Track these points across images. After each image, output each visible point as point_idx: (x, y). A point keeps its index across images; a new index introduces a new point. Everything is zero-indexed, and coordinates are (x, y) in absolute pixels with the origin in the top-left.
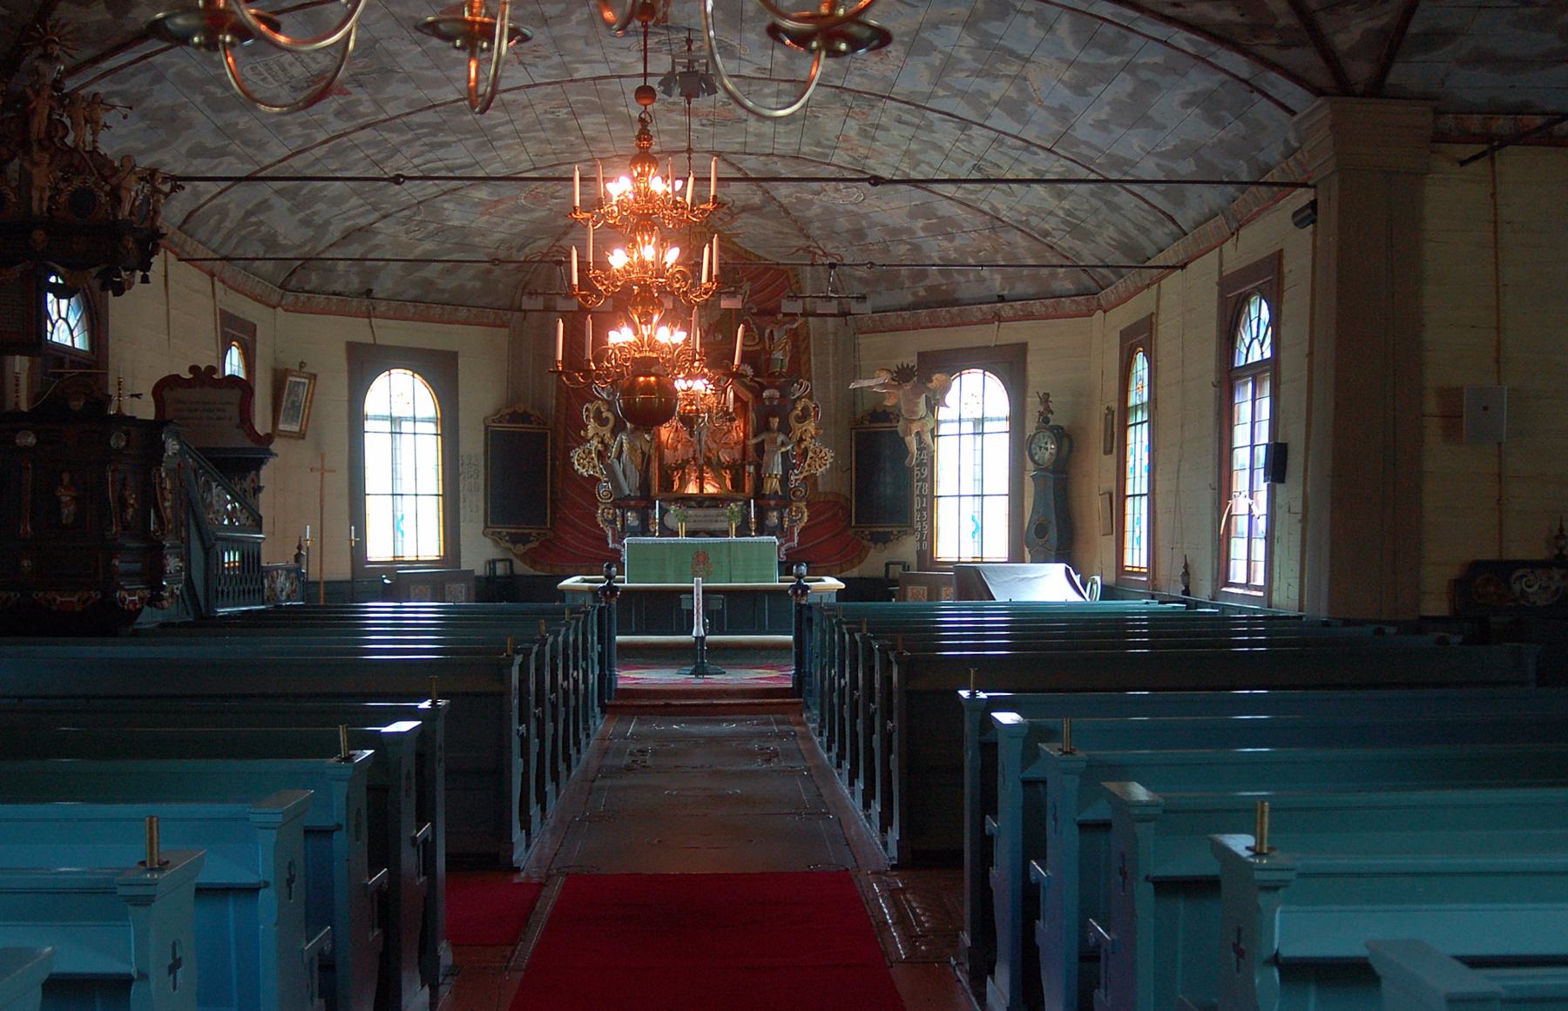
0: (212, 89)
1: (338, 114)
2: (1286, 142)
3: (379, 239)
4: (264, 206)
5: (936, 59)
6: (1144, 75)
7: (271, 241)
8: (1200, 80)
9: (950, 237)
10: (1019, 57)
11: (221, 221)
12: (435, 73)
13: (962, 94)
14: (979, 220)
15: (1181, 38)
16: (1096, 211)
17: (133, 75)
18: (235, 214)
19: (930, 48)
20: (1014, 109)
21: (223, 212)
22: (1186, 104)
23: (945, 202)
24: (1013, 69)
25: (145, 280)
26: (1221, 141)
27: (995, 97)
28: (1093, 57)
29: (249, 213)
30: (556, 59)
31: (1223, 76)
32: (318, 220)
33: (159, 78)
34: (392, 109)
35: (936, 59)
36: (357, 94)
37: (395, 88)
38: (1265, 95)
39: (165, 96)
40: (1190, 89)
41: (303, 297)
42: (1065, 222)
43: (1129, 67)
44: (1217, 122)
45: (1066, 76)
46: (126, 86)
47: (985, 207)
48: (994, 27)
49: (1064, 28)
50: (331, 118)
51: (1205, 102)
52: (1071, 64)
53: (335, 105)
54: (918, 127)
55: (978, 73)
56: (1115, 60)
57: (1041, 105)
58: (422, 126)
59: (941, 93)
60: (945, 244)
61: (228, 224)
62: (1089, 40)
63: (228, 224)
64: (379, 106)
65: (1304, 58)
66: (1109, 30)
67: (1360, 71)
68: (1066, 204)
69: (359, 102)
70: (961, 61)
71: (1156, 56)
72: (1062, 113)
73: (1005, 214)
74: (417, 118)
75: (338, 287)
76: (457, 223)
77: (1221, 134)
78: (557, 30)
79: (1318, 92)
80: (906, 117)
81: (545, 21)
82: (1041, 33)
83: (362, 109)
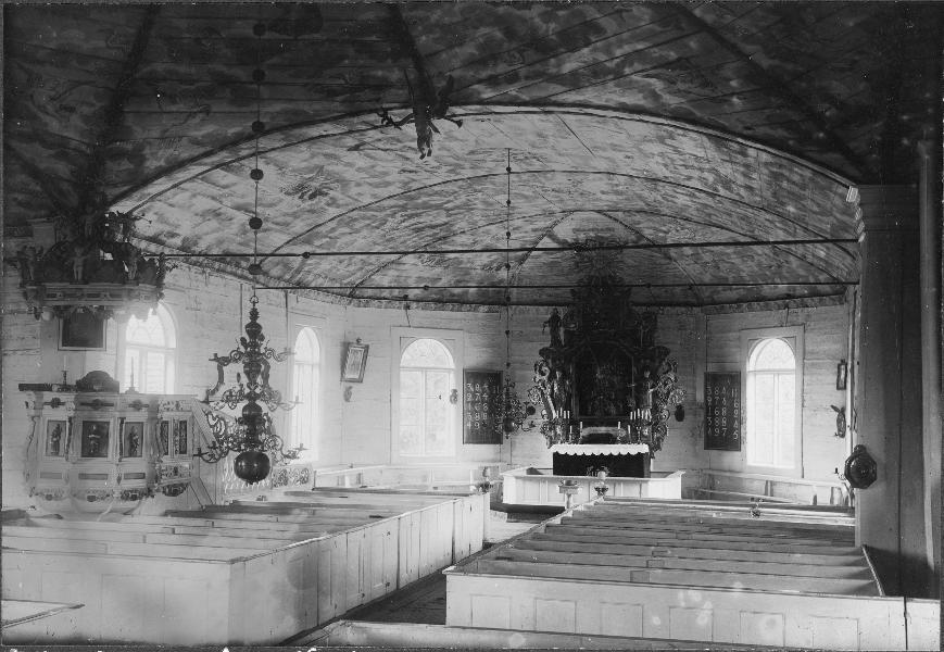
60: (750, 263)
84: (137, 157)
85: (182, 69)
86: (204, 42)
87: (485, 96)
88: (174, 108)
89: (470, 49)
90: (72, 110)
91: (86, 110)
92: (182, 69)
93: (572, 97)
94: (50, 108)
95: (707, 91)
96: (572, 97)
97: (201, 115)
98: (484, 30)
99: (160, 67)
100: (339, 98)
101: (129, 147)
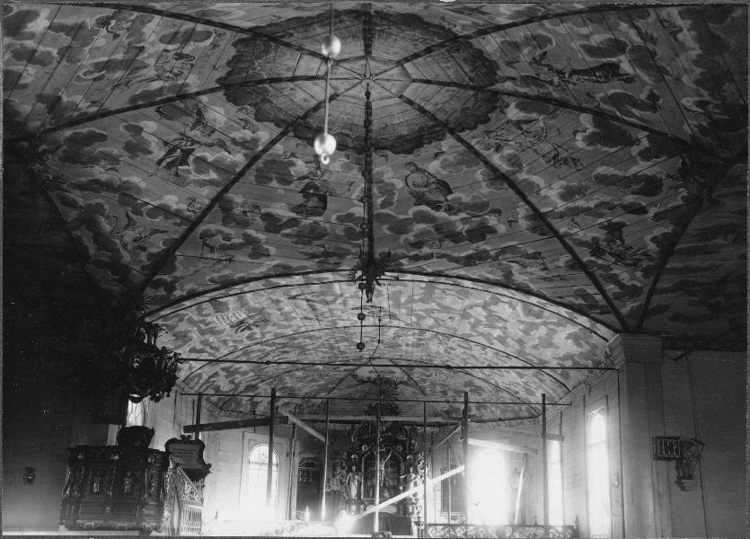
0: (201, 325)
1: (247, 338)
2: (606, 353)
3: (259, 391)
4: (216, 374)
5: (472, 320)
6: (551, 327)
7: (217, 389)
8: (571, 329)
9: (480, 395)
10: (503, 320)
11: (200, 379)
12: (285, 323)
13: (482, 334)
14: (490, 388)
15: (563, 311)
16: (535, 383)
17: (172, 318)
18: (205, 377)
19: (469, 316)
20: (502, 340)
21: (200, 376)
22: (567, 338)
23: (477, 380)
24: (501, 325)
25: (168, 396)
26: (581, 353)
27: (495, 335)
28: (531, 319)
29: (210, 377)
30: (331, 319)
31: (581, 327)
32: (236, 381)
33: (181, 320)
34: (268, 337)
35: (472, 320)
36: (256, 330)
37: (269, 328)
38: (597, 334)
39: (182, 327)
40: (568, 332)
41: (228, 413)
42: (524, 388)
43: (545, 324)
44: (579, 345)
45: (521, 327)
46: (168, 323)
47: (493, 382)
48: (493, 308)
49: (519, 307)
50: (245, 339)
51: (576, 338)
52: (523, 322)
53: (246, 334)
54: (466, 348)
55: (486, 326)
56: (539, 321)
57: (513, 339)
58: (279, 344)
59: (474, 334)
61: (201, 381)
62: (528, 312)
63: (201, 381)
64: (263, 335)
65: (610, 318)
66: (536, 309)
67: (631, 322)
68: (524, 380)
69: (255, 333)
70: (482, 321)
71: (555, 319)
72: (520, 342)
73: (500, 385)
74: (277, 341)
75: (242, 409)
76: (290, 385)
77: (580, 350)
78: (332, 306)
79: (616, 331)
80: (462, 344)
81: (327, 303)
82: (511, 310)
83: (256, 336)
84: (170, 287)
85: (227, 230)
86: (248, 214)
87: (405, 267)
88: (210, 256)
89: (410, 237)
90: (144, 249)
91: (154, 250)
92: (227, 230)
93: (462, 272)
94: (130, 247)
95: (543, 274)
96: (462, 272)
97: (225, 263)
98: (421, 226)
99: (213, 227)
100: (317, 260)
101: (167, 278)
